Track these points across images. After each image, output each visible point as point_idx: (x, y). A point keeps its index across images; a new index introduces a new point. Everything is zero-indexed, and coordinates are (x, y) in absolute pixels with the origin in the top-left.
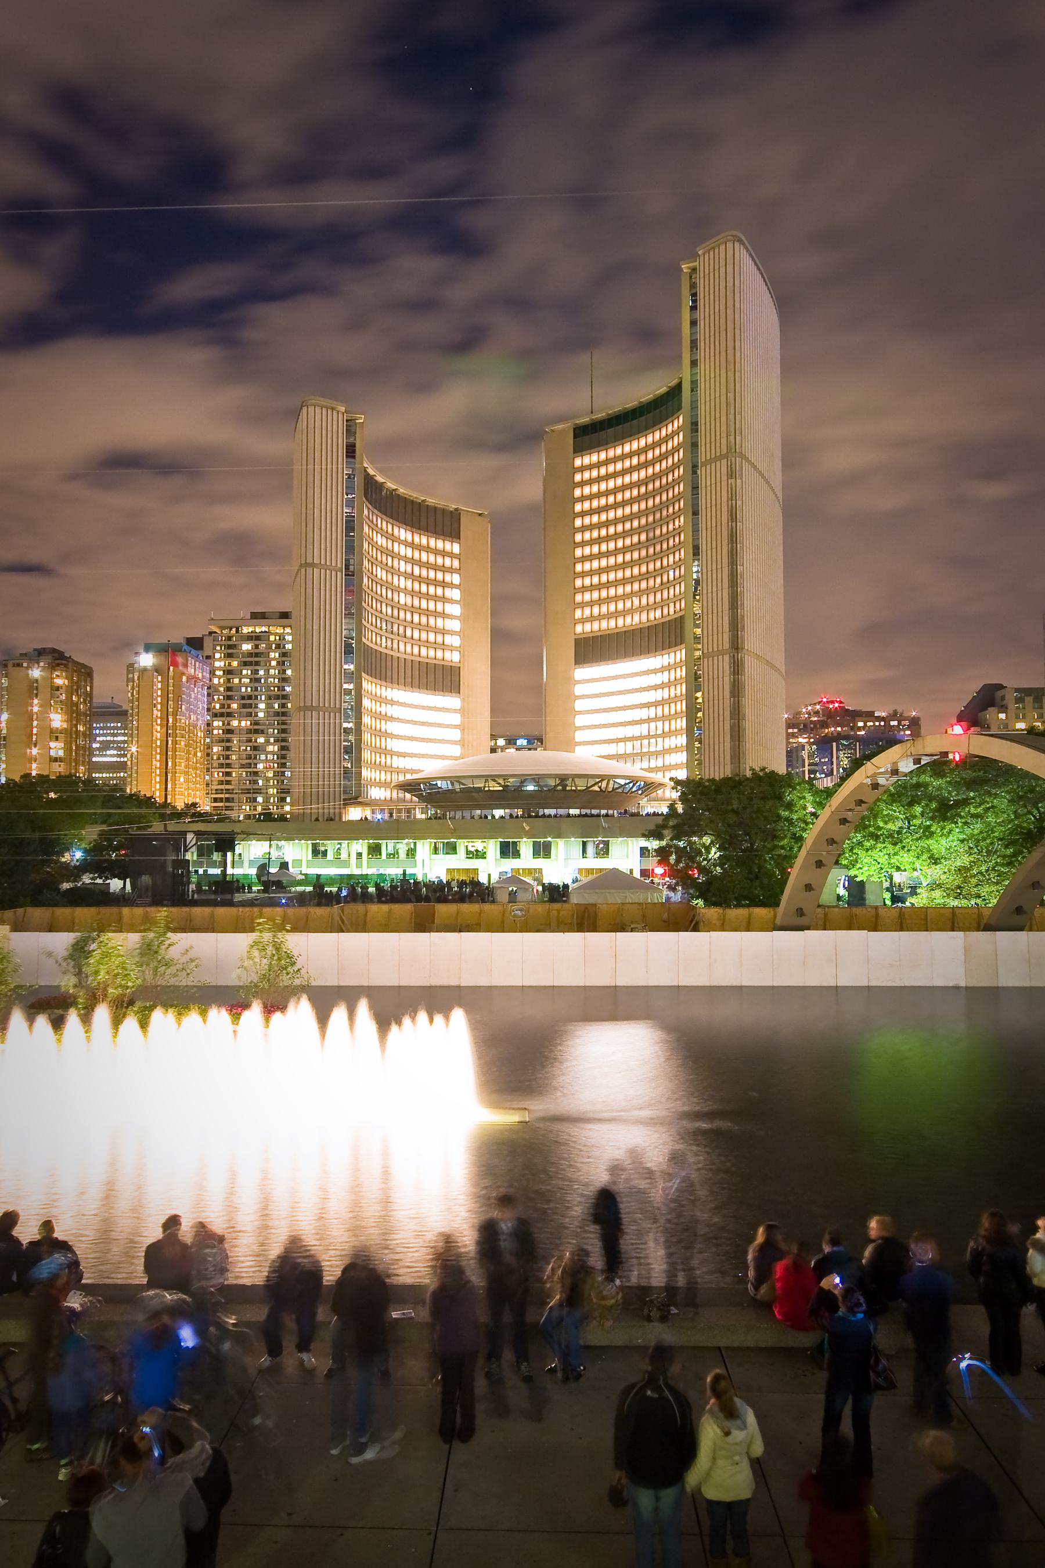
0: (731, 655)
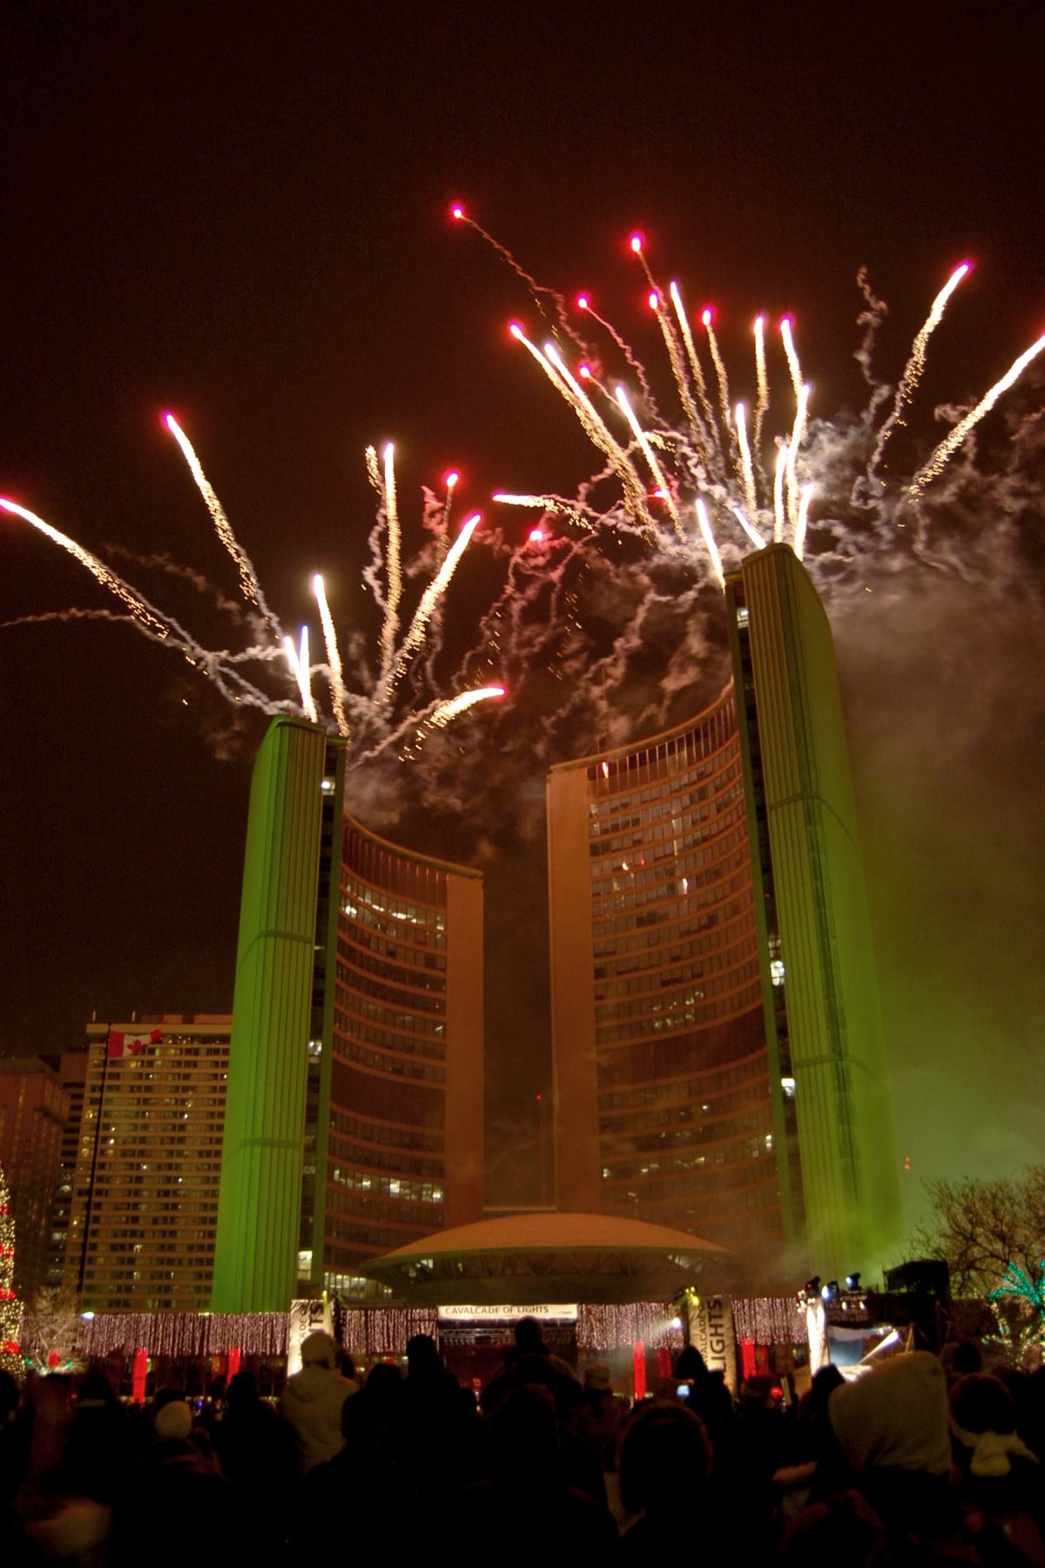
0: (834, 1063)
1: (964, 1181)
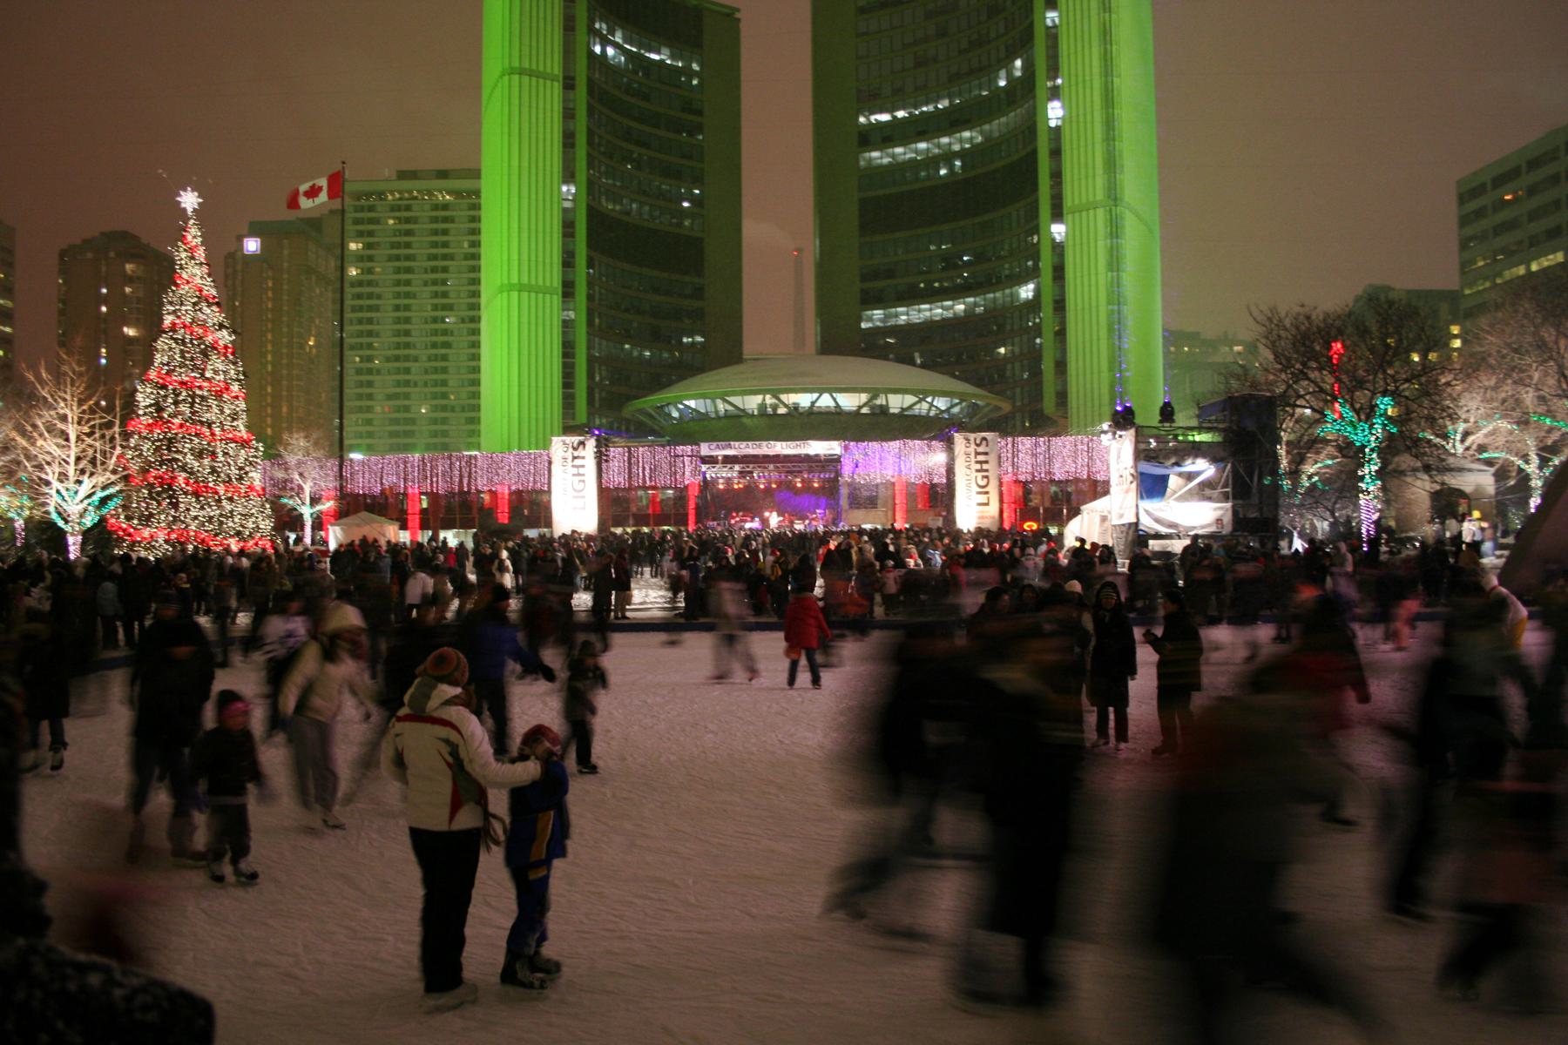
1: (1297, 309)
